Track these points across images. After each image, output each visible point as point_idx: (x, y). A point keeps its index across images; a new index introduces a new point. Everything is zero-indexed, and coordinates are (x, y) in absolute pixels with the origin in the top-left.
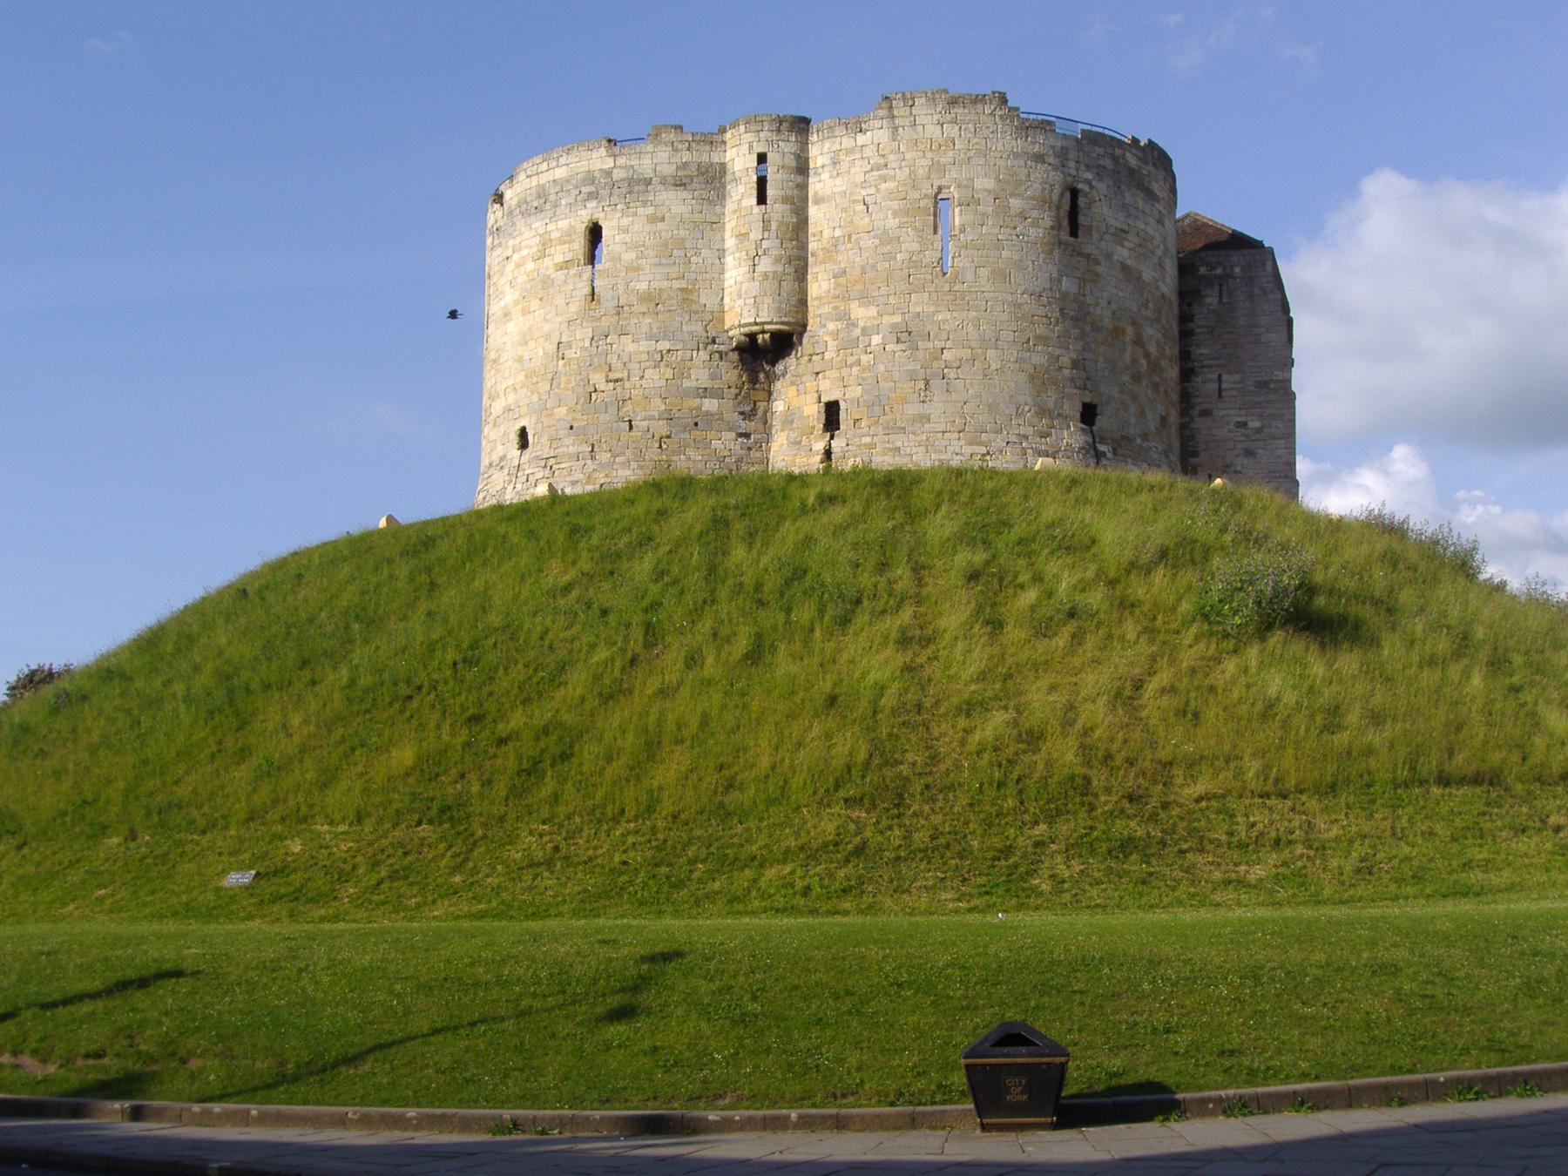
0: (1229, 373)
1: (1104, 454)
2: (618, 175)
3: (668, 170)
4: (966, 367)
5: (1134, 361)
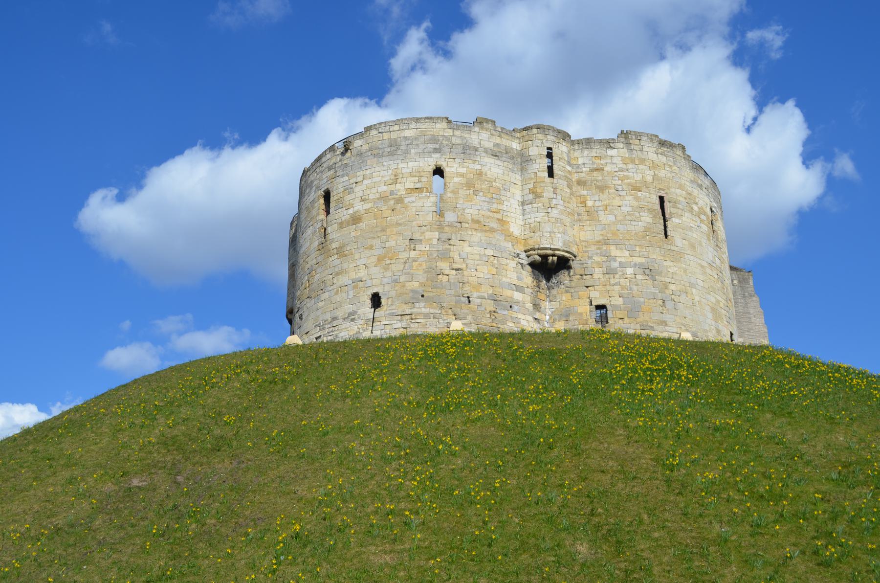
2: (455, 140)
3: (489, 145)
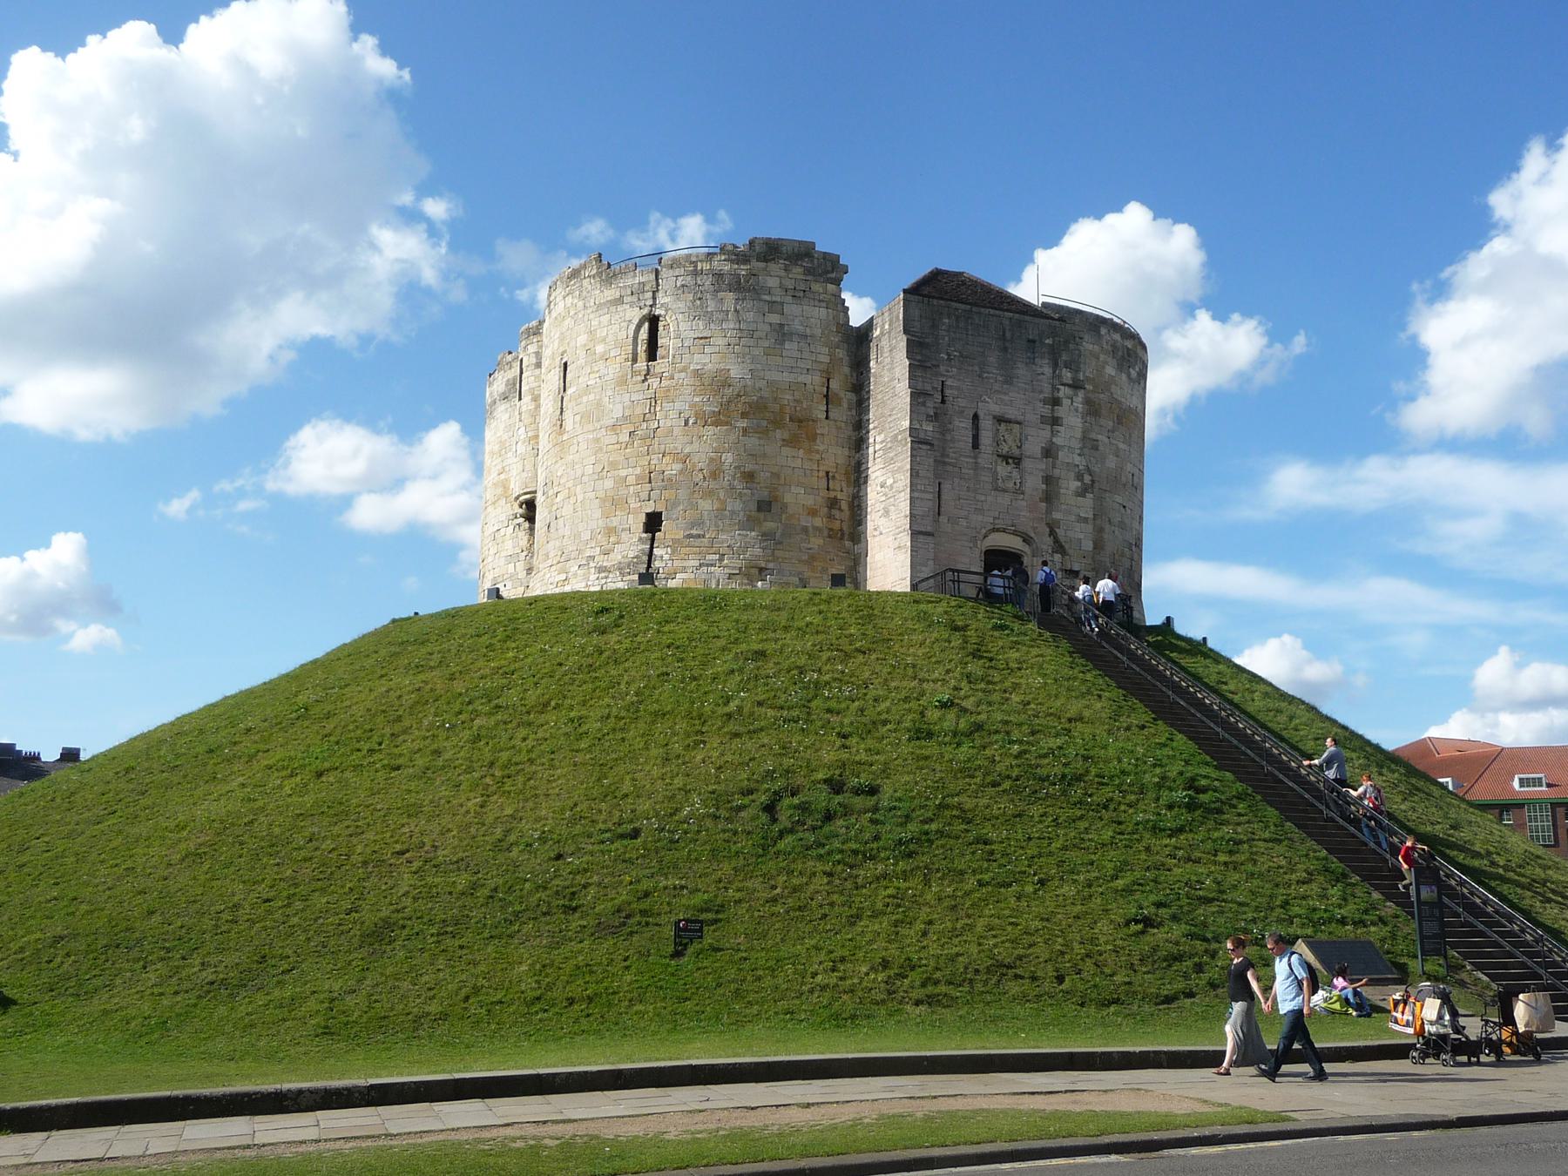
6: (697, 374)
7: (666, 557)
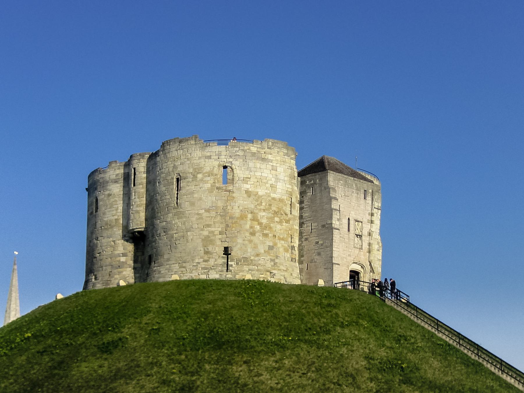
0: (314, 223)
1: (232, 266)
4: (182, 239)
5: (251, 227)
6: (247, 192)
7: (233, 266)
